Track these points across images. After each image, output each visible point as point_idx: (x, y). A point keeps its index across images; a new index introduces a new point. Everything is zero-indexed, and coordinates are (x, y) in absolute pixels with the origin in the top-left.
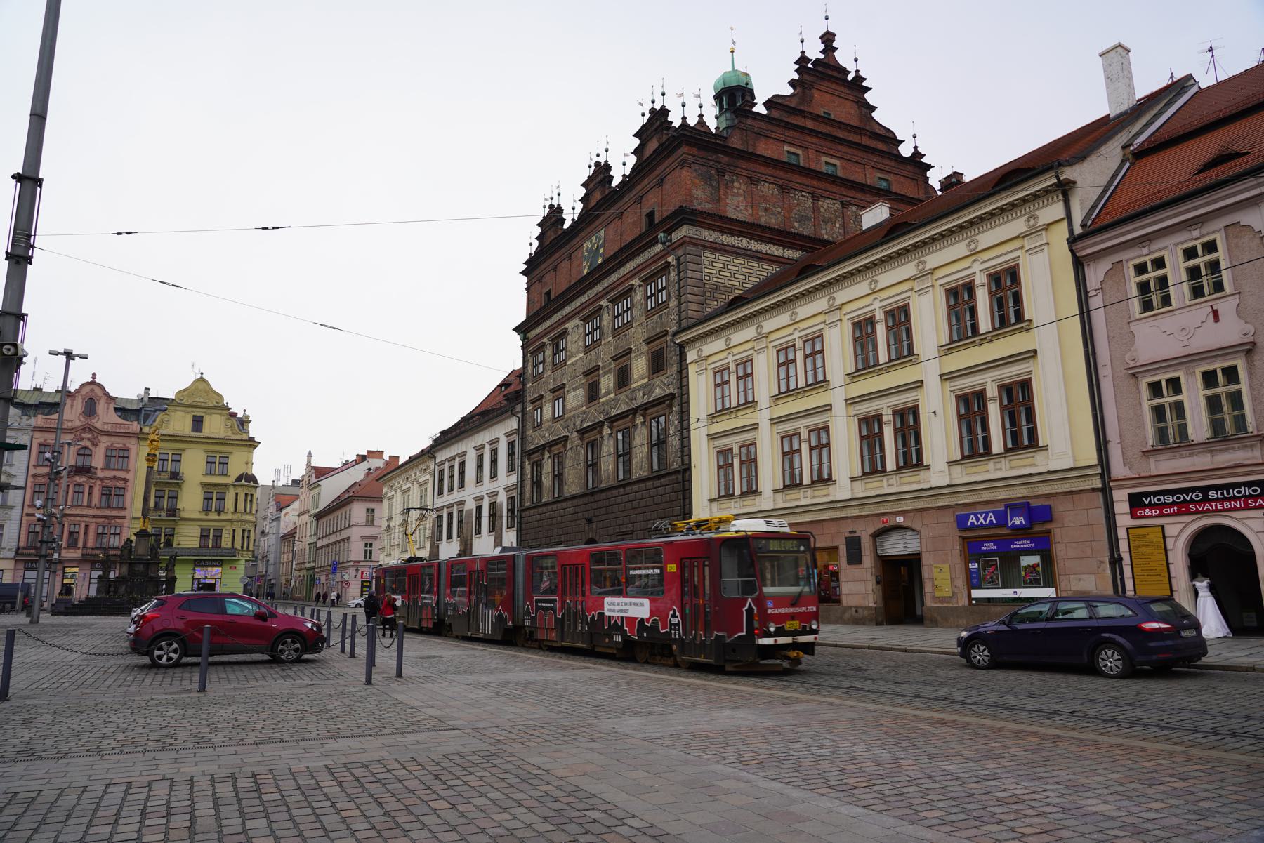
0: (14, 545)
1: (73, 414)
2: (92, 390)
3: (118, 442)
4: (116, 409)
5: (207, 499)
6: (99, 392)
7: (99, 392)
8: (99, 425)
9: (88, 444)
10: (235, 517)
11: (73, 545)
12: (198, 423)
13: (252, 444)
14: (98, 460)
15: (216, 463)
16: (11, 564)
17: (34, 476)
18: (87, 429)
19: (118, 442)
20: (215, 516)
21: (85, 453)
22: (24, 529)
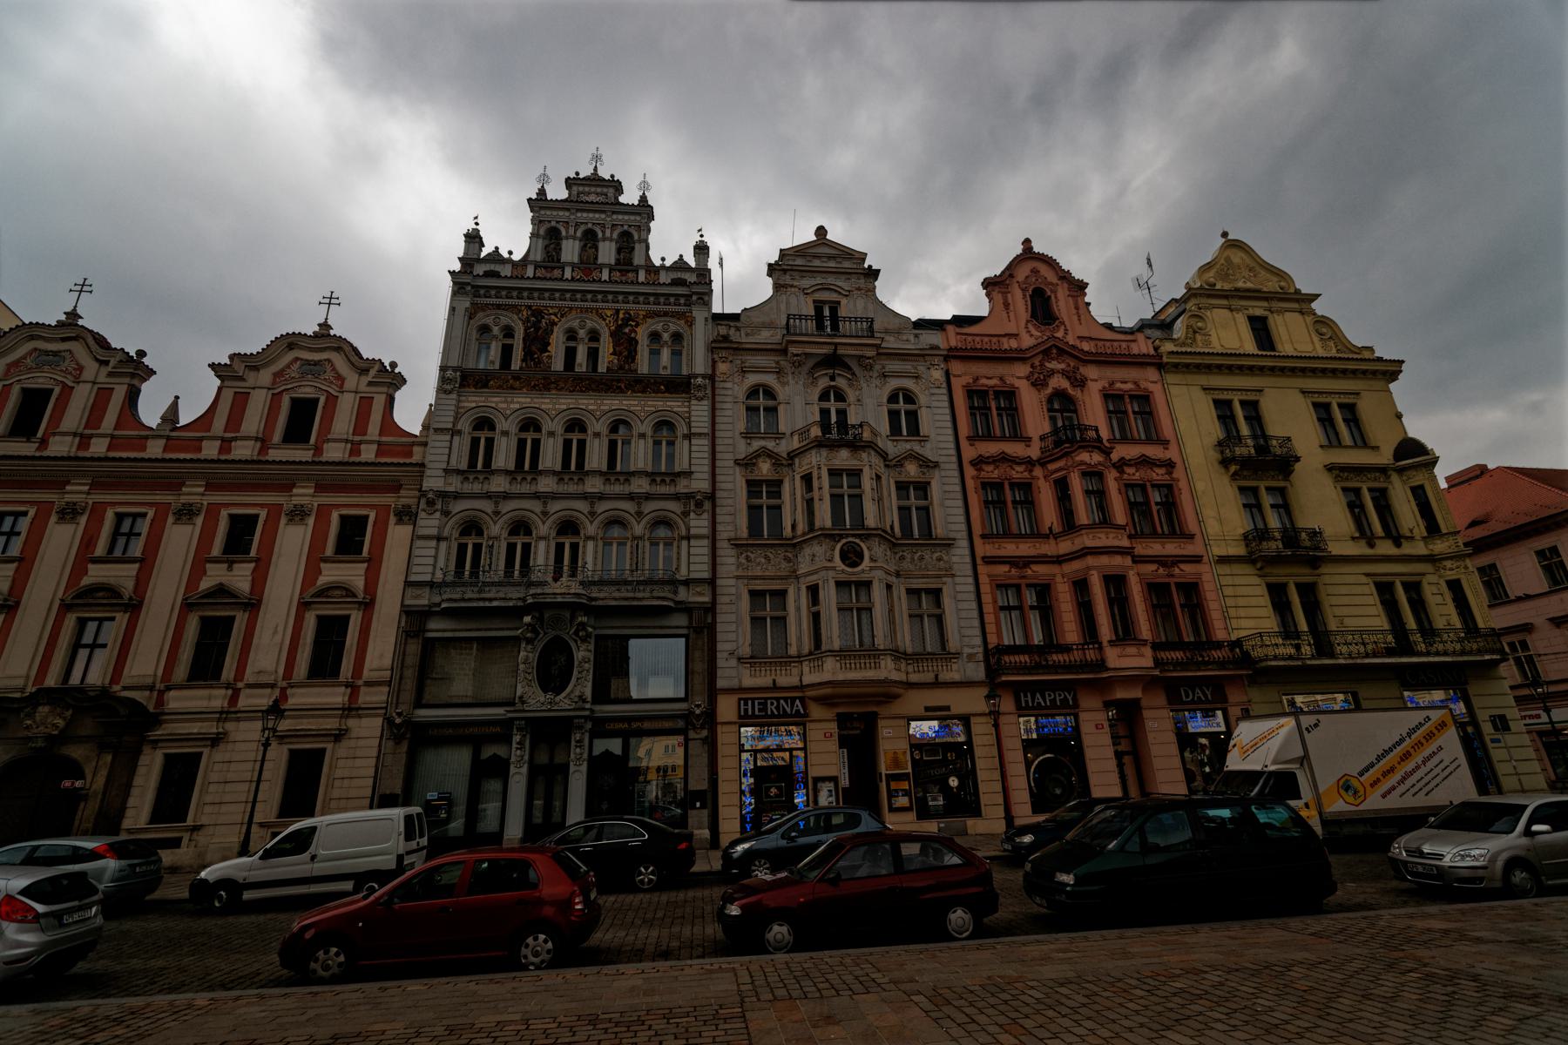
0: (978, 641)
2: (1035, 271)
3: (1124, 380)
5: (1355, 506)
6: (1051, 277)
7: (1051, 277)
8: (1071, 340)
9: (1065, 384)
10: (1439, 547)
11: (1126, 633)
13: (1390, 371)
15: (1339, 420)
16: (973, 701)
17: (978, 462)
19: (1124, 380)
20: (1386, 548)
21: (1062, 404)
22: (987, 599)
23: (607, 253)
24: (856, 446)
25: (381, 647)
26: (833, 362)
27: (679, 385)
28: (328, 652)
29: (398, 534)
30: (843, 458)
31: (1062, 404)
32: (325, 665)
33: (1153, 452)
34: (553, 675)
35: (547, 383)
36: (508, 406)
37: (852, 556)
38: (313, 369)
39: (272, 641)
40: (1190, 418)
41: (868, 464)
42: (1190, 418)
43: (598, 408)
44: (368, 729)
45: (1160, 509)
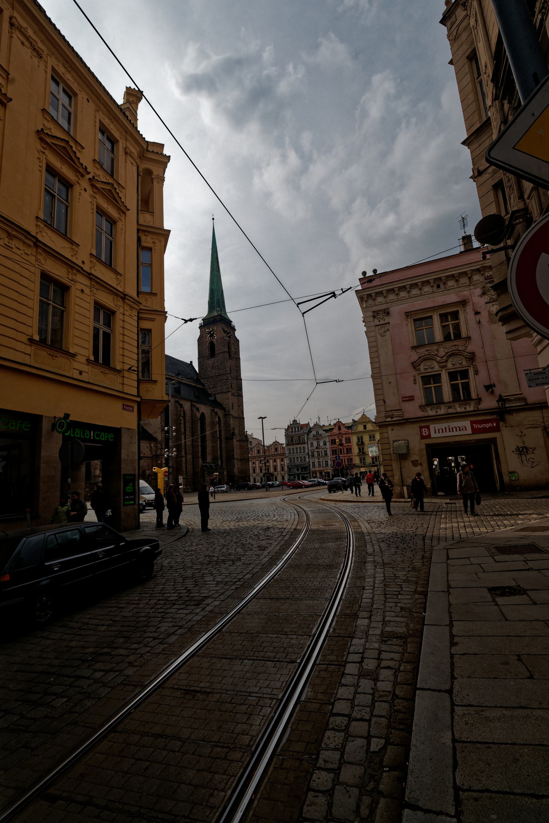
1: (336, 431)
3: (347, 436)
4: (345, 427)
12: (365, 427)
14: (344, 442)
18: (339, 434)
19: (347, 436)
21: (341, 440)
23: (297, 430)
24: (319, 449)
25: (286, 469)
26: (318, 439)
27: (304, 443)
28: (283, 469)
29: (285, 459)
30: (318, 450)
31: (341, 440)
32: (283, 470)
33: (349, 444)
34: (298, 470)
35: (294, 445)
36: (291, 447)
37: (319, 459)
38: (276, 445)
39: (279, 468)
40: (354, 440)
41: (320, 450)
42: (354, 440)
43: (298, 446)
44: (286, 475)
45: (349, 450)
